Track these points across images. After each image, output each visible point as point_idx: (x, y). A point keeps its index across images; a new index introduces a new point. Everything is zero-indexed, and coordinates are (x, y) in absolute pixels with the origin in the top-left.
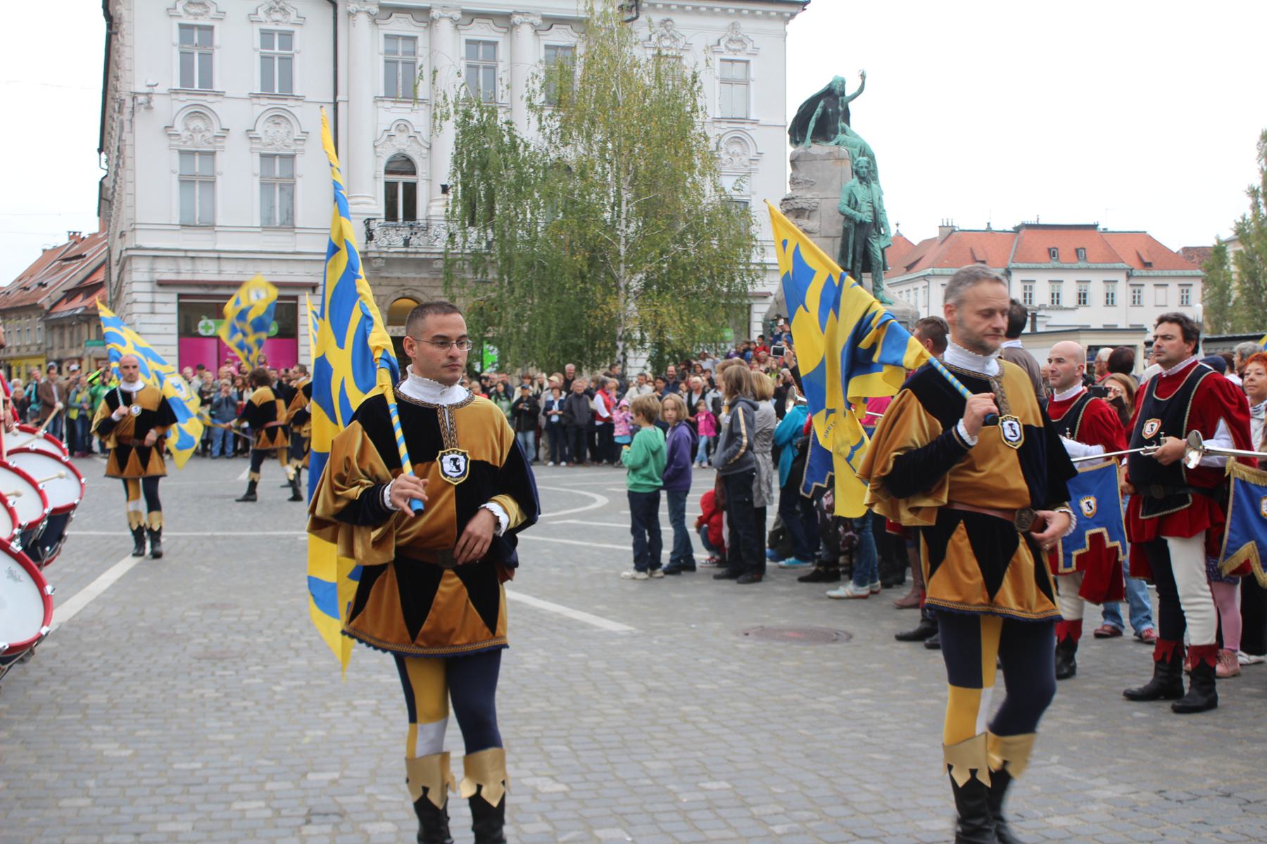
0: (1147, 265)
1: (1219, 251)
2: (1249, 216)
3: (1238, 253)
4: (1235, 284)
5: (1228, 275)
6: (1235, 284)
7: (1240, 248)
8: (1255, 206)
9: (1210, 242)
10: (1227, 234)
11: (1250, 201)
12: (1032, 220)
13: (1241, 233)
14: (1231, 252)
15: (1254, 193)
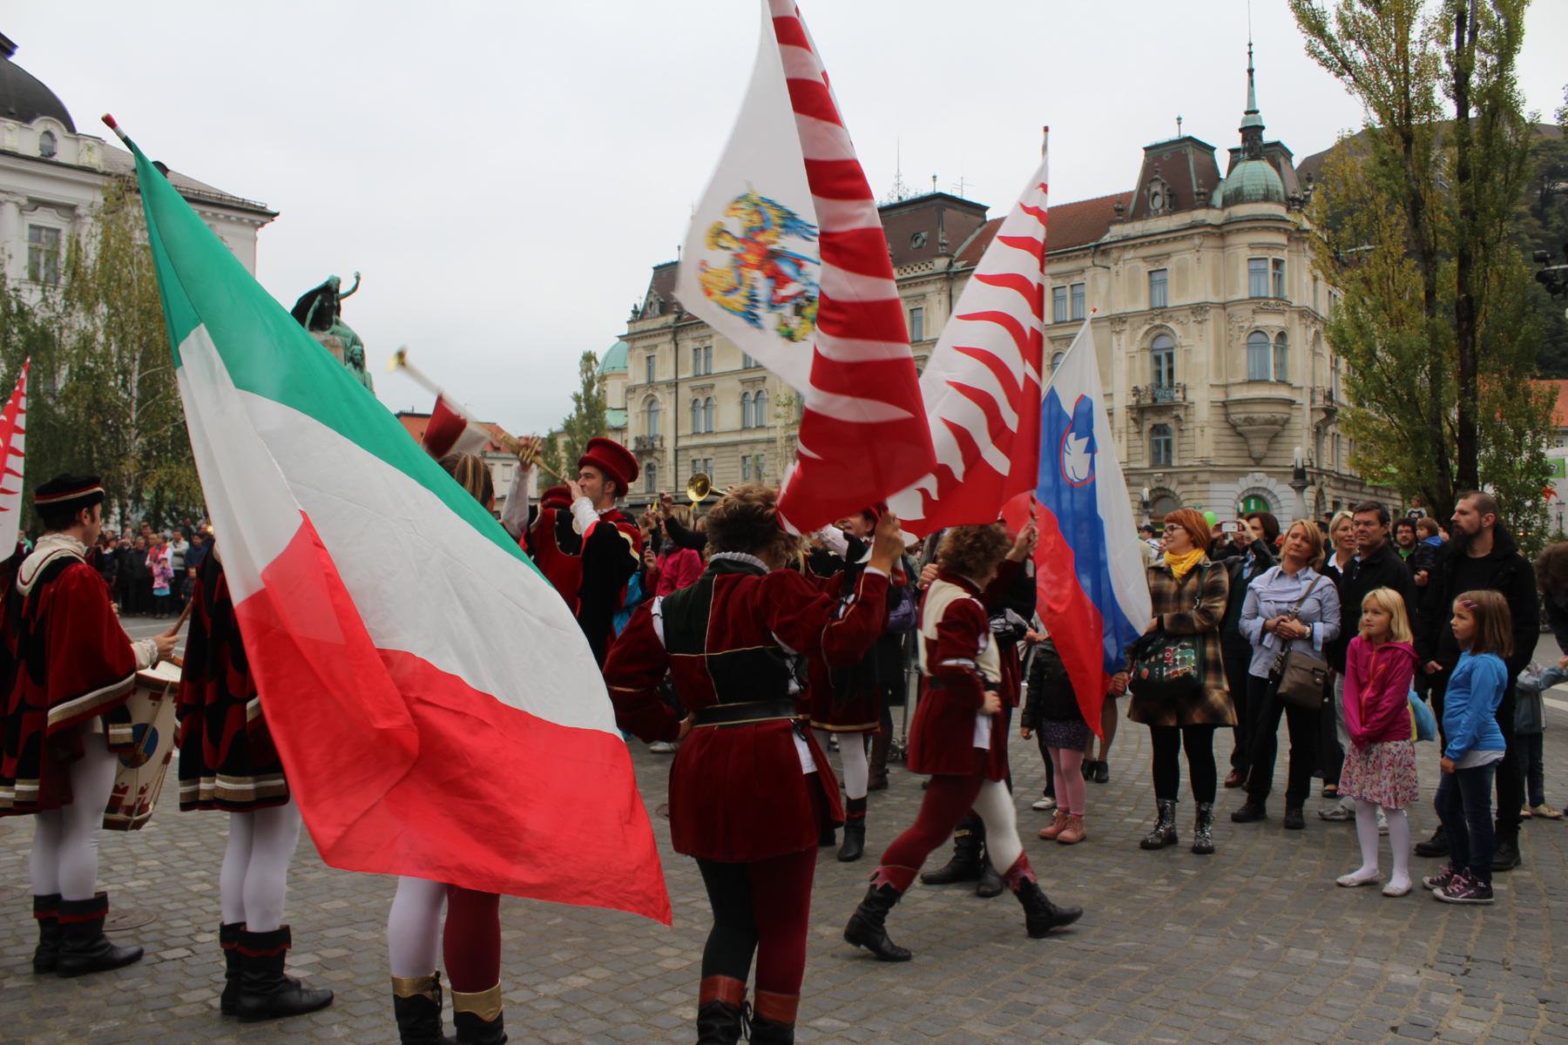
0: (497, 449)
1: (551, 441)
2: (574, 415)
3: (567, 443)
4: (564, 467)
5: (558, 460)
6: (564, 467)
7: (567, 438)
8: (579, 409)
9: (544, 434)
10: (558, 426)
11: (575, 404)
12: (408, 410)
13: (569, 427)
14: (561, 442)
15: (577, 398)
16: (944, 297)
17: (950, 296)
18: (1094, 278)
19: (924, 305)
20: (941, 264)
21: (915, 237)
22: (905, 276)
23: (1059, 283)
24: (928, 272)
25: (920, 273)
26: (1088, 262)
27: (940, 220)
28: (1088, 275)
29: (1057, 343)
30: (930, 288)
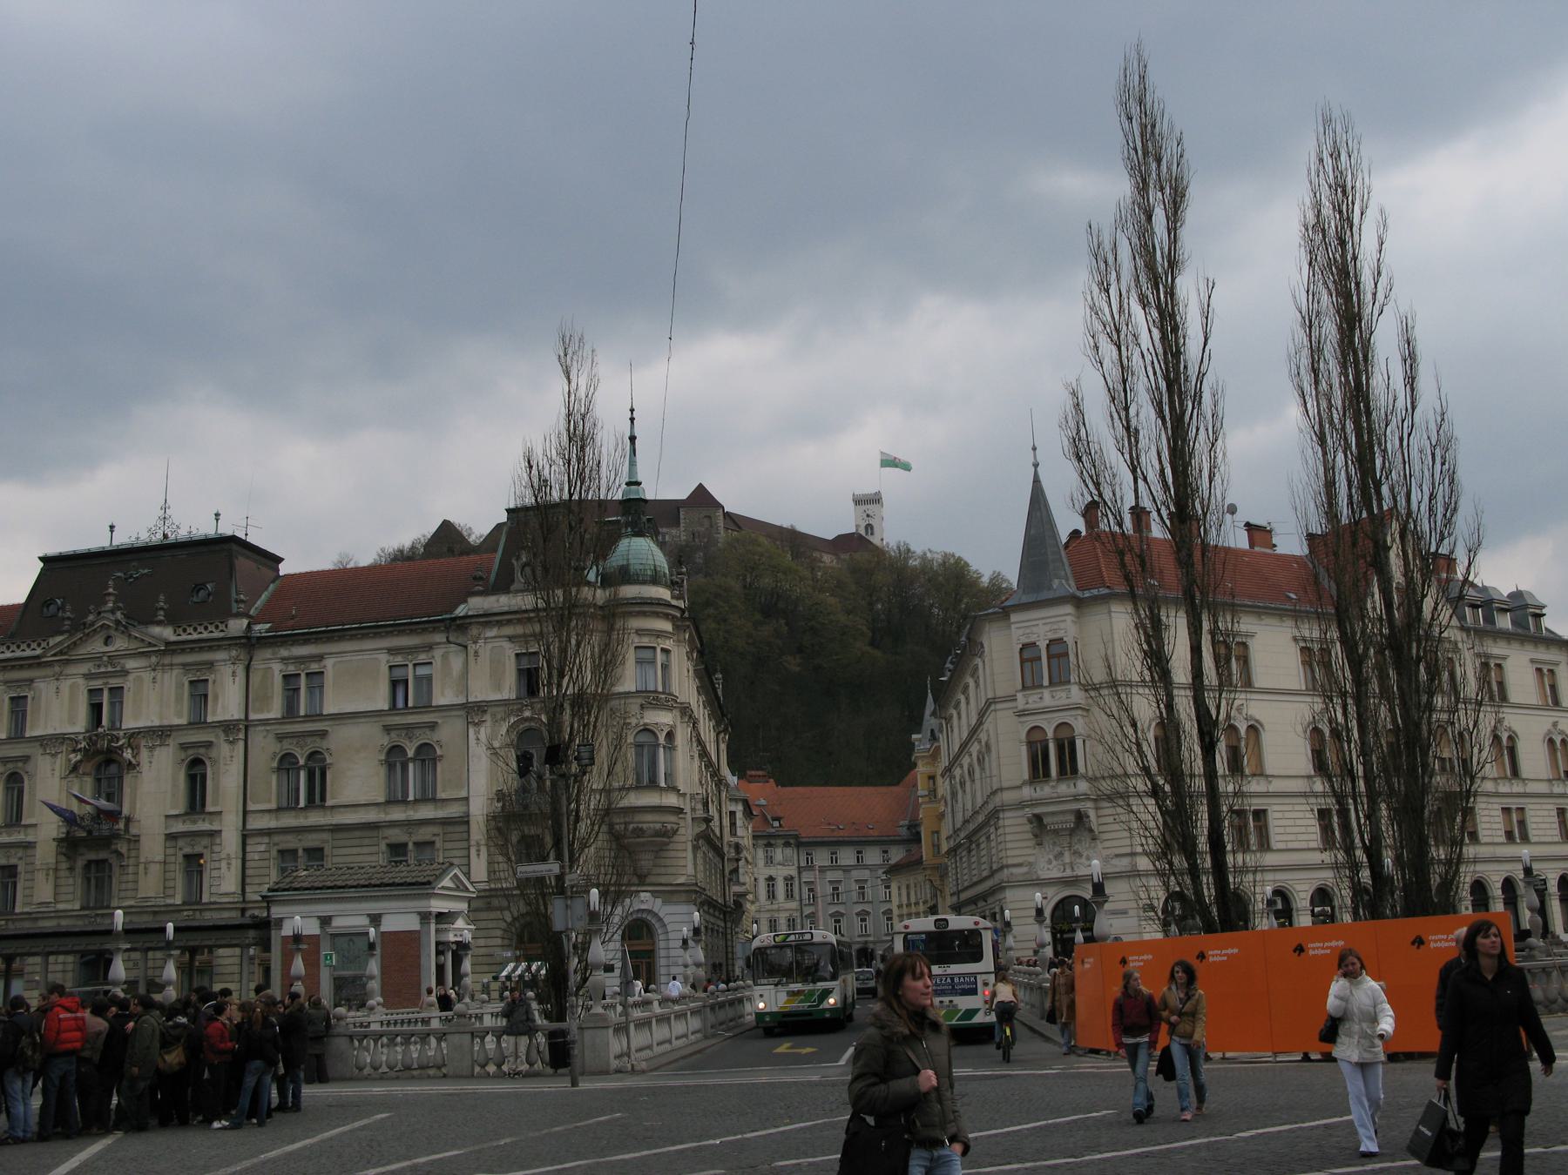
16: (240, 670)
17: (248, 669)
18: (445, 657)
19: (211, 678)
20: (237, 626)
21: (199, 587)
22: (184, 637)
23: (399, 660)
24: (217, 634)
25: (205, 635)
26: (439, 637)
27: (232, 568)
28: (438, 653)
29: (393, 734)
30: (220, 655)
